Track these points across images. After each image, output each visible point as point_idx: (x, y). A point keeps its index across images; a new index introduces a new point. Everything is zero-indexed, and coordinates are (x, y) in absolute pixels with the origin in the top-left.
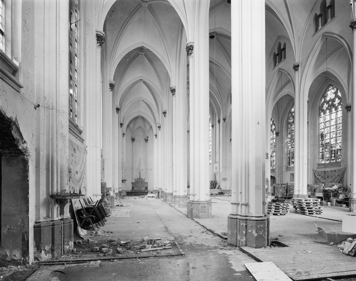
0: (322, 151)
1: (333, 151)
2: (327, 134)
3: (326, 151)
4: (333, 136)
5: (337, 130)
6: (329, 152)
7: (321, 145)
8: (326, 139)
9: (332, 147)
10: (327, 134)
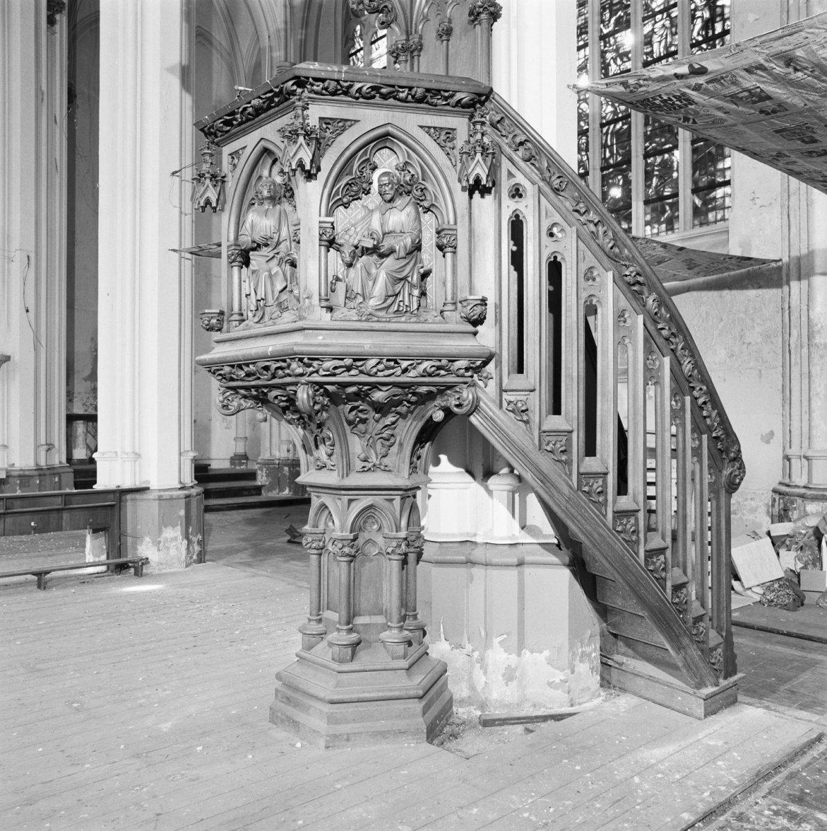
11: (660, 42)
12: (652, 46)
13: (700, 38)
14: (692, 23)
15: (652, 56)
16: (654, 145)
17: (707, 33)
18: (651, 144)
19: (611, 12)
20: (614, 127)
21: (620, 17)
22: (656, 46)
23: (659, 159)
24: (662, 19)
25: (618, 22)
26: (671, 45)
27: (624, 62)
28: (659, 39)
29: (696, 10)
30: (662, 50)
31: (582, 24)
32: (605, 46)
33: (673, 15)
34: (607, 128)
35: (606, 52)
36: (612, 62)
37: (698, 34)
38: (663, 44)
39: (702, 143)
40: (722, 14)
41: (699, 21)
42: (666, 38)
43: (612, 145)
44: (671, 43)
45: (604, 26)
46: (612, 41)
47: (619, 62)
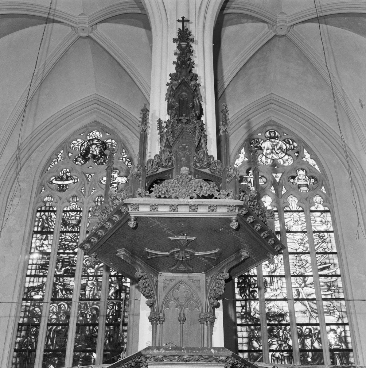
0: (250, 343)
1: (310, 354)
2: (268, 279)
3: (274, 347)
4: (299, 294)
5: (320, 273)
6: (285, 354)
7: (242, 317)
8: (267, 296)
9: (301, 335)
10: (268, 279)
11: (90, 291)
12: (85, 292)
13: (113, 298)
14: (109, 288)
15: (85, 297)
16: (80, 345)
17: (117, 296)
18: (78, 344)
19: (63, 265)
20: (56, 328)
21: (68, 269)
22: (87, 292)
23: (83, 355)
24: (92, 280)
25: (66, 271)
26: (96, 295)
27: (67, 294)
28: (90, 289)
29: (112, 282)
30: (91, 295)
31: (43, 264)
32: (56, 281)
33: (99, 280)
34: (51, 327)
35: (57, 284)
36: (60, 291)
37: (112, 295)
38: (92, 292)
39: (109, 353)
40: (125, 290)
41: (113, 288)
42: (94, 290)
43: (53, 338)
44: (96, 294)
45: (57, 270)
46: (61, 280)
47: (64, 292)
